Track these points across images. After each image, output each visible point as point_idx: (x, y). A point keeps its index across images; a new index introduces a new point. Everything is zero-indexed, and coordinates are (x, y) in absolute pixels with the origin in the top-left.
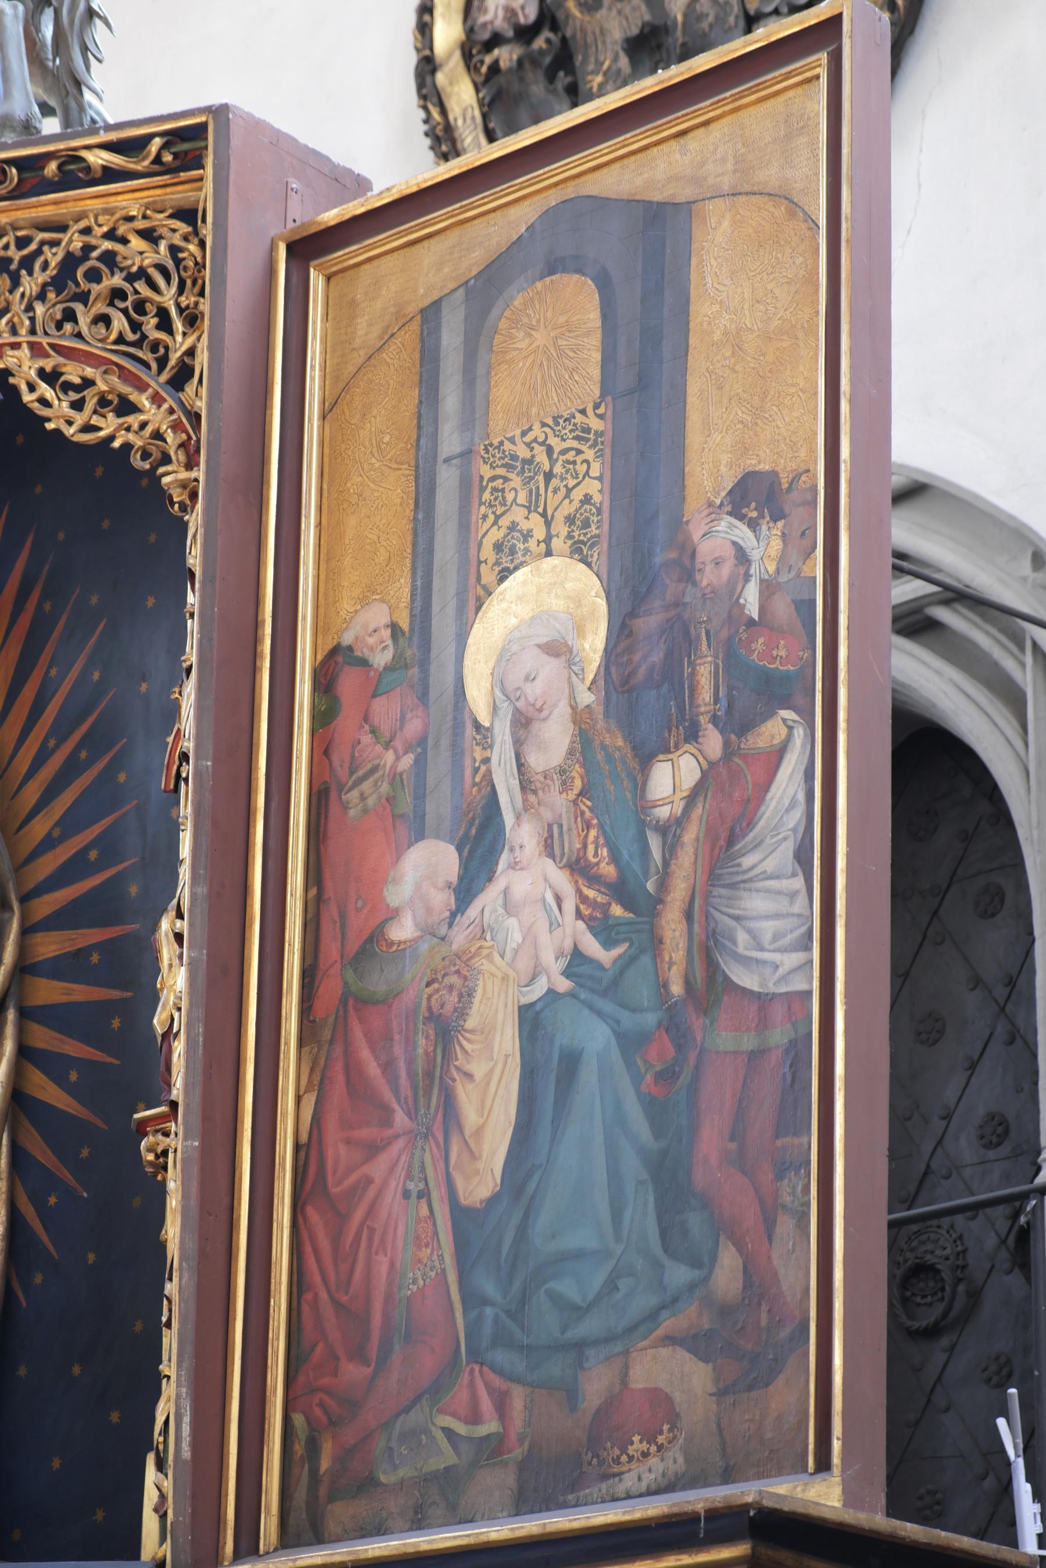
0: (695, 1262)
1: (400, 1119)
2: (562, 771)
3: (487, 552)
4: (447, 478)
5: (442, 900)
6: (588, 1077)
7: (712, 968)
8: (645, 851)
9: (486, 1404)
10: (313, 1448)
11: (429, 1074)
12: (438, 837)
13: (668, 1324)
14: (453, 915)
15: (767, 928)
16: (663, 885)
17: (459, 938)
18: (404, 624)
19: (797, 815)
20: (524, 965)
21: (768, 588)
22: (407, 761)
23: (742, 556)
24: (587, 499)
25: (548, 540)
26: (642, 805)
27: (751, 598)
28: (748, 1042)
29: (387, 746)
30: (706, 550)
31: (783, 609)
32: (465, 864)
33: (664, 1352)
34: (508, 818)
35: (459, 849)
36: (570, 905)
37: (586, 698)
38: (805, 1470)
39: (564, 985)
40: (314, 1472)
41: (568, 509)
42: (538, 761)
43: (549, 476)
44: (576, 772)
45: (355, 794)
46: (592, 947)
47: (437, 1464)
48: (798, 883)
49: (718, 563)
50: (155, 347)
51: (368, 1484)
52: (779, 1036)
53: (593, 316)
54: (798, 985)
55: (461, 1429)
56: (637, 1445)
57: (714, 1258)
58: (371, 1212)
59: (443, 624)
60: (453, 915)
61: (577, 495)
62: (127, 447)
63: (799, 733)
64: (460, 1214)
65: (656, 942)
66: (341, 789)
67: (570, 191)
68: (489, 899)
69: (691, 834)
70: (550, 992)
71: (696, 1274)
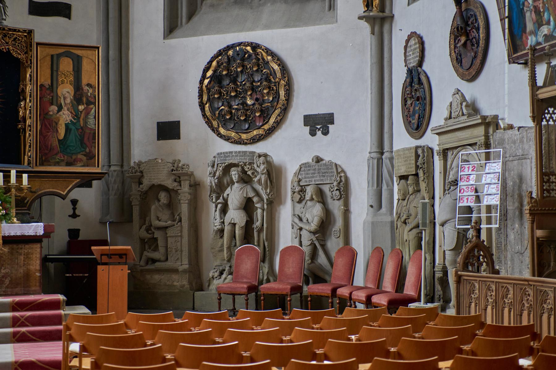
0: (84, 148)
1: (51, 130)
2: (69, 104)
3: (60, 81)
4: (55, 73)
5: (56, 112)
6: (72, 131)
7: (86, 125)
8: (79, 113)
9: (62, 156)
10: (42, 158)
11: (55, 127)
12: (55, 105)
13: (81, 153)
14: (57, 114)
15: (91, 123)
16: (80, 116)
17: (58, 115)
18: (50, 84)
19: (94, 114)
20: (65, 119)
21: (91, 94)
22: (51, 98)
23: (88, 90)
24: (71, 80)
25: (67, 82)
26: (78, 110)
27: (89, 94)
28: (89, 132)
29: (49, 95)
30: (84, 89)
31: (92, 96)
32: (58, 109)
33: (82, 155)
34: (63, 106)
35: (58, 107)
36: (70, 115)
37: (72, 98)
38: (95, 166)
39: (70, 122)
40: (42, 160)
41: (69, 80)
42: (66, 102)
43: (67, 76)
44: (71, 104)
45: (44, 99)
46: (73, 120)
47: (56, 161)
48: (94, 120)
49: (86, 90)
50: (23, 49)
51: (49, 161)
52: (92, 132)
53: (72, 63)
54: (94, 128)
55: (59, 158)
56: (79, 162)
57: (86, 149)
58: (48, 137)
59: (55, 86)
60: (57, 114)
61: (70, 79)
62: (20, 58)
63: (94, 108)
64: (59, 141)
65: (79, 121)
66: (43, 98)
67: (68, 50)
68: (61, 113)
69: (83, 113)
70: (68, 123)
71: (84, 150)
